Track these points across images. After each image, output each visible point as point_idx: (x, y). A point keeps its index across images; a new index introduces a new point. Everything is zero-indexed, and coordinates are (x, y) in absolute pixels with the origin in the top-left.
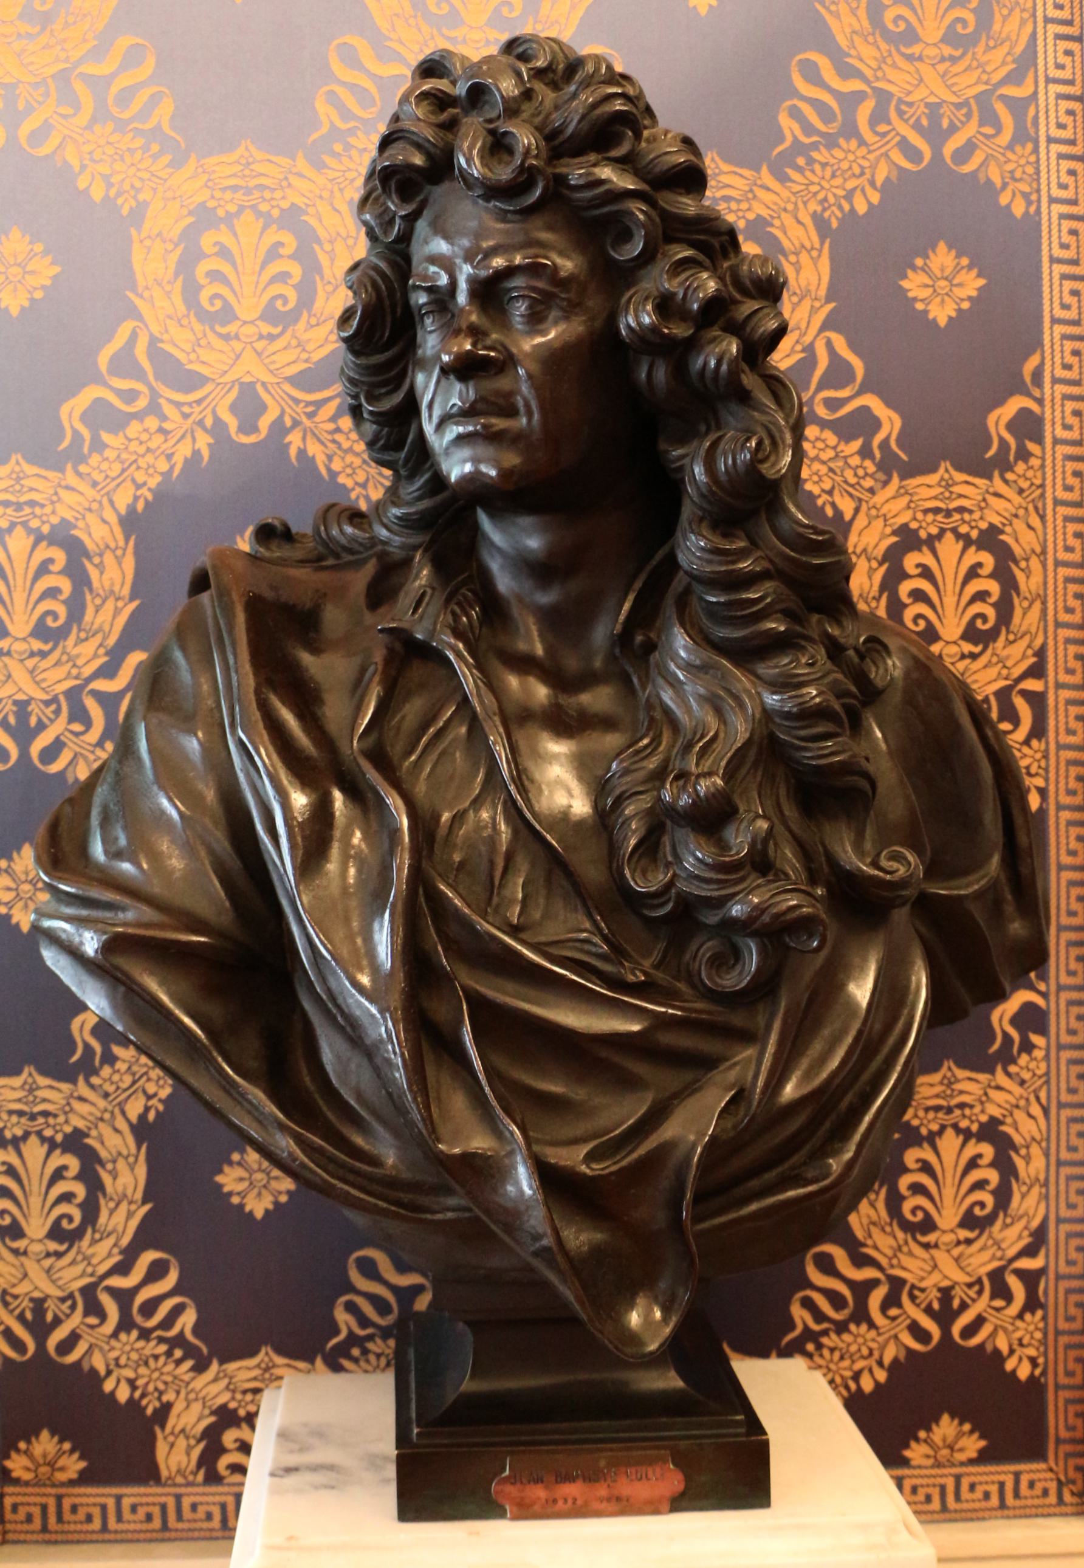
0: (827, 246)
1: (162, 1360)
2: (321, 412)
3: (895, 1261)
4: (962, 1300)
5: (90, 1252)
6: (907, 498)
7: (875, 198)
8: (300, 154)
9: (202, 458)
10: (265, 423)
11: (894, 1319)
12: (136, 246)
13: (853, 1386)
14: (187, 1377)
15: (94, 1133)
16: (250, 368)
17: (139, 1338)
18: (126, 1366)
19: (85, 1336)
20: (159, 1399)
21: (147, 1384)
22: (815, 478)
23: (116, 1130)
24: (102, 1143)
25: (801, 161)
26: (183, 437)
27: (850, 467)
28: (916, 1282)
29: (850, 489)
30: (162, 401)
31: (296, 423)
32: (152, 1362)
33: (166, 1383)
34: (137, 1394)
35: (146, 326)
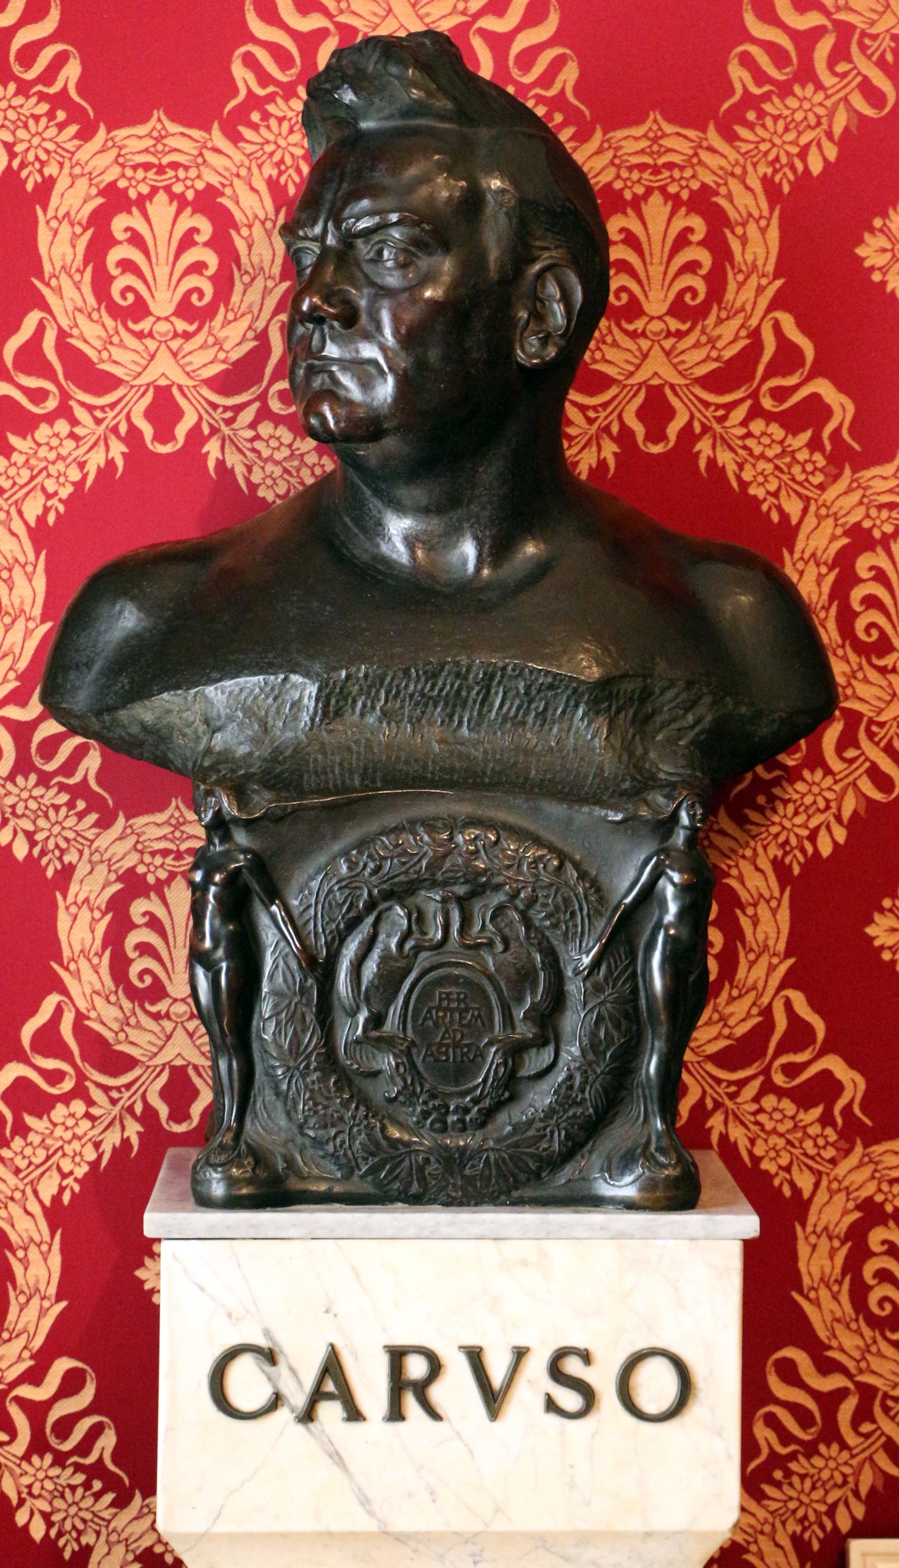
0: (776, 213)
2: (239, 419)
6: (860, 492)
7: (832, 153)
8: (216, 125)
9: (116, 469)
10: (181, 430)
12: (42, 226)
16: (163, 369)
22: (760, 479)
25: (751, 116)
26: (95, 444)
27: (798, 462)
30: (72, 403)
31: (214, 431)
35: (54, 318)
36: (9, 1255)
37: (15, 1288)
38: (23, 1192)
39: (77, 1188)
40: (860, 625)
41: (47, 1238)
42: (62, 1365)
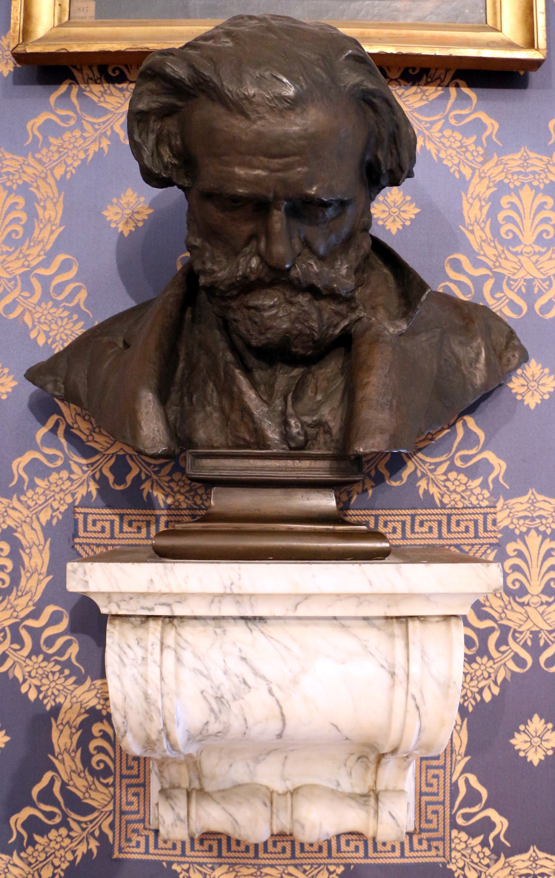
1: (57, 675)
3: (503, 615)
4: (546, 641)
5: (15, 603)
11: (503, 653)
13: (478, 698)
14: (71, 688)
15: (19, 530)
17: (43, 661)
18: (35, 677)
19: (11, 655)
20: (54, 700)
21: (48, 689)
23: (33, 529)
24: (24, 536)
28: (516, 628)
29: (471, 164)
32: (50, 676)
33: (59, 690)
34: (41, 696)
36: (21, 552)
37: (24, 569)
38: (31, 518)
39: (60, 517)
40: (503, 230)
41: (42, 542)
42: (50, 609)
